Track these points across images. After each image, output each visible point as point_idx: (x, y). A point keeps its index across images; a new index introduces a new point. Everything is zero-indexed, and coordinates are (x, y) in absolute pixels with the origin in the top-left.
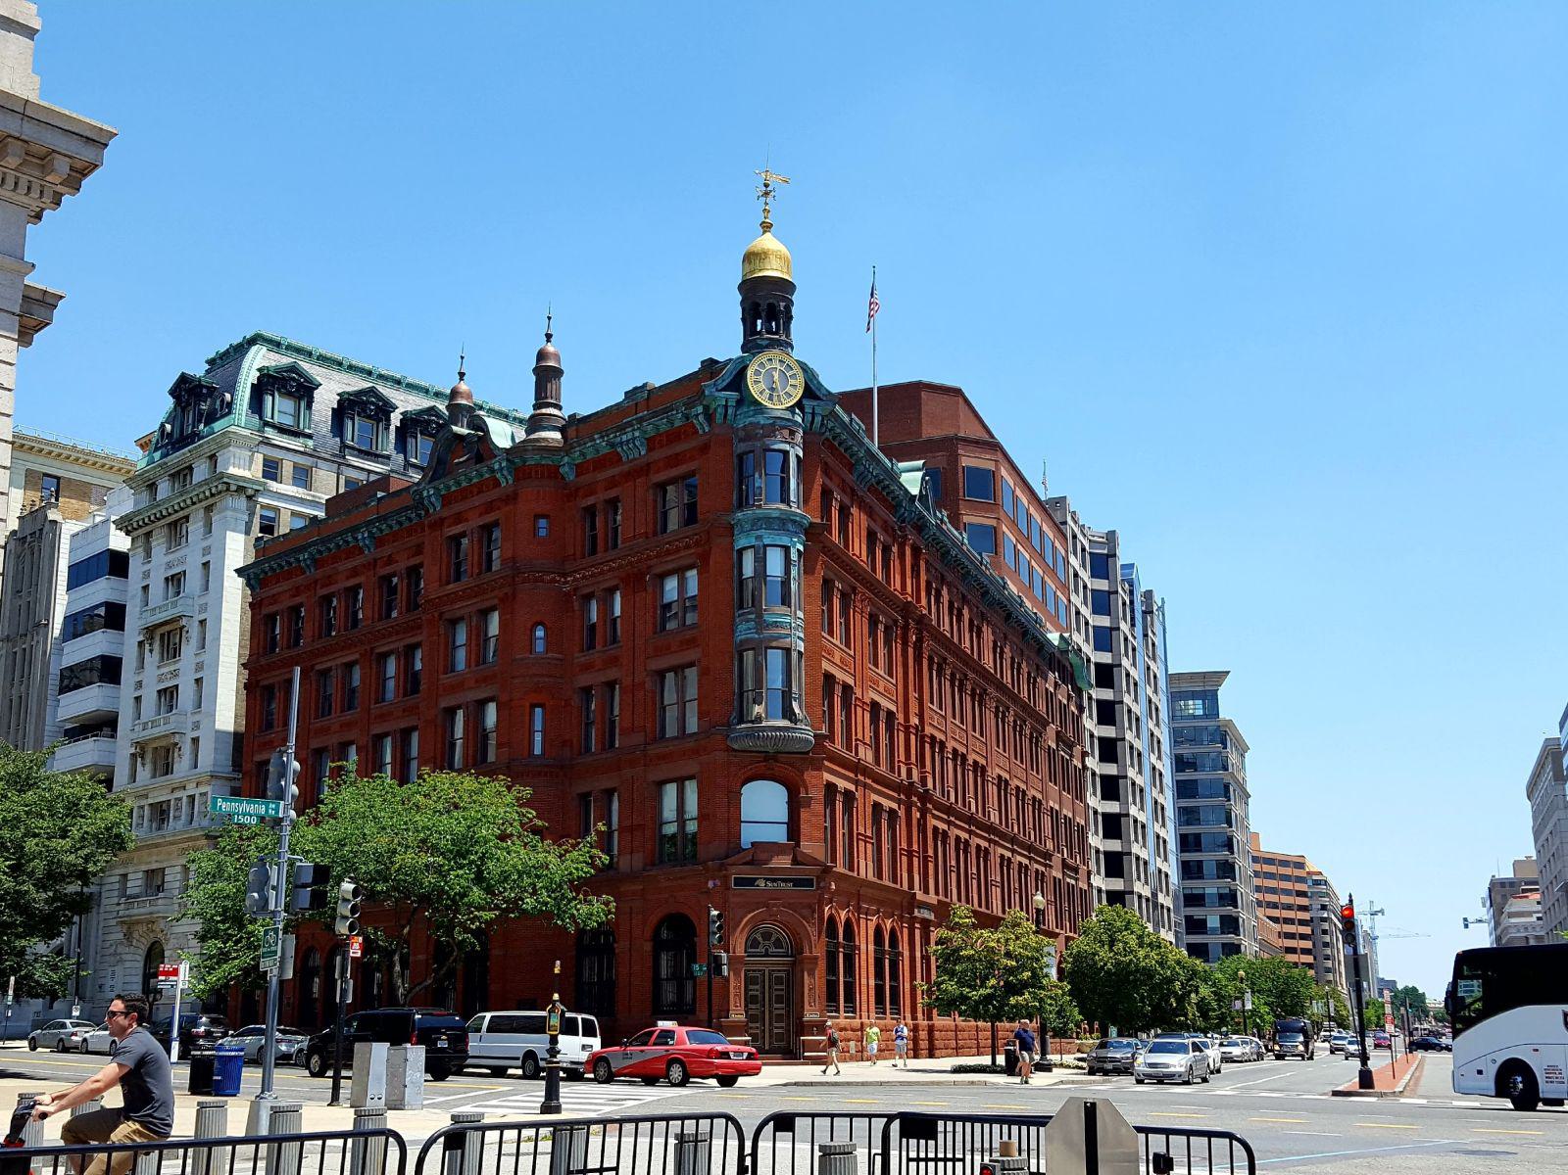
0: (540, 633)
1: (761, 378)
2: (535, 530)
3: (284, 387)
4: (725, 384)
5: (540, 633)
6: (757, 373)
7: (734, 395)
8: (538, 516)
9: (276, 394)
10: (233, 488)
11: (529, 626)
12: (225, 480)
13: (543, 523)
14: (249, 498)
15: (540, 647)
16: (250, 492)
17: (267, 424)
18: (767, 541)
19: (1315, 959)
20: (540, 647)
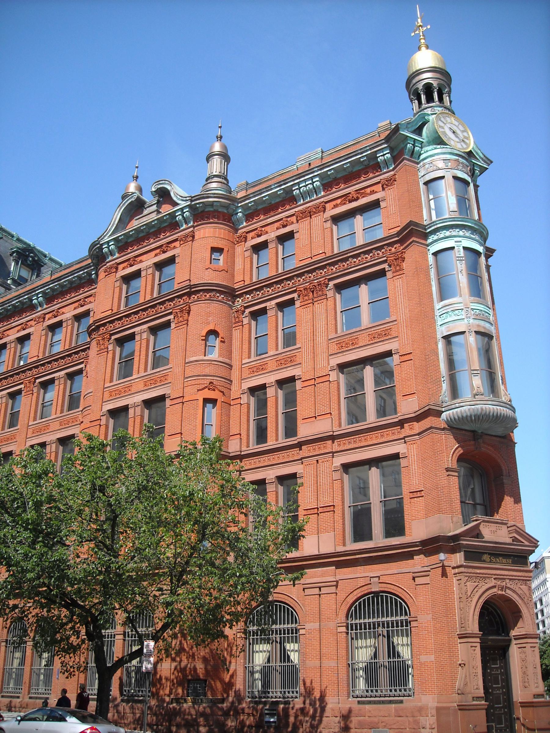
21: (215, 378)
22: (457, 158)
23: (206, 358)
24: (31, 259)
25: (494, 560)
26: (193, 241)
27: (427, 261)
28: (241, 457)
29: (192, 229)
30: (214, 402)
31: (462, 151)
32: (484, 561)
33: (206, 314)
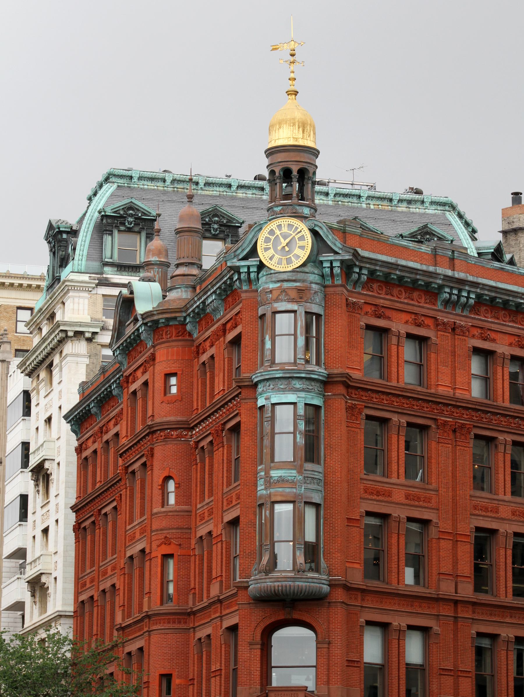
0: (171, 486)
1: (270, 245)
2: (166, 388)
3: (123, 224)
4: (245, 252)
5: (171, 486)
6: (267, 240)
7: (253, 262)
8: (168, 376)
9: (116, 232)
10: (70, 334)
11: (160, 482)
12: (62, 328)
13: (173, 381)
14: (89, 340)
15: (172, 500)
16: (88, 335)
17: (106, 264)
18: (274, 400)
20: (172, 500)
21: (170, 531)
22: (278, 285)
23: (163, 510)
24: (216, 226)
26: (154, 365)
27: (256, 417)
28: (194, 613)
29: (152, 350)
30: (171, 556)
31: (290, 269)
33: (165, 456)
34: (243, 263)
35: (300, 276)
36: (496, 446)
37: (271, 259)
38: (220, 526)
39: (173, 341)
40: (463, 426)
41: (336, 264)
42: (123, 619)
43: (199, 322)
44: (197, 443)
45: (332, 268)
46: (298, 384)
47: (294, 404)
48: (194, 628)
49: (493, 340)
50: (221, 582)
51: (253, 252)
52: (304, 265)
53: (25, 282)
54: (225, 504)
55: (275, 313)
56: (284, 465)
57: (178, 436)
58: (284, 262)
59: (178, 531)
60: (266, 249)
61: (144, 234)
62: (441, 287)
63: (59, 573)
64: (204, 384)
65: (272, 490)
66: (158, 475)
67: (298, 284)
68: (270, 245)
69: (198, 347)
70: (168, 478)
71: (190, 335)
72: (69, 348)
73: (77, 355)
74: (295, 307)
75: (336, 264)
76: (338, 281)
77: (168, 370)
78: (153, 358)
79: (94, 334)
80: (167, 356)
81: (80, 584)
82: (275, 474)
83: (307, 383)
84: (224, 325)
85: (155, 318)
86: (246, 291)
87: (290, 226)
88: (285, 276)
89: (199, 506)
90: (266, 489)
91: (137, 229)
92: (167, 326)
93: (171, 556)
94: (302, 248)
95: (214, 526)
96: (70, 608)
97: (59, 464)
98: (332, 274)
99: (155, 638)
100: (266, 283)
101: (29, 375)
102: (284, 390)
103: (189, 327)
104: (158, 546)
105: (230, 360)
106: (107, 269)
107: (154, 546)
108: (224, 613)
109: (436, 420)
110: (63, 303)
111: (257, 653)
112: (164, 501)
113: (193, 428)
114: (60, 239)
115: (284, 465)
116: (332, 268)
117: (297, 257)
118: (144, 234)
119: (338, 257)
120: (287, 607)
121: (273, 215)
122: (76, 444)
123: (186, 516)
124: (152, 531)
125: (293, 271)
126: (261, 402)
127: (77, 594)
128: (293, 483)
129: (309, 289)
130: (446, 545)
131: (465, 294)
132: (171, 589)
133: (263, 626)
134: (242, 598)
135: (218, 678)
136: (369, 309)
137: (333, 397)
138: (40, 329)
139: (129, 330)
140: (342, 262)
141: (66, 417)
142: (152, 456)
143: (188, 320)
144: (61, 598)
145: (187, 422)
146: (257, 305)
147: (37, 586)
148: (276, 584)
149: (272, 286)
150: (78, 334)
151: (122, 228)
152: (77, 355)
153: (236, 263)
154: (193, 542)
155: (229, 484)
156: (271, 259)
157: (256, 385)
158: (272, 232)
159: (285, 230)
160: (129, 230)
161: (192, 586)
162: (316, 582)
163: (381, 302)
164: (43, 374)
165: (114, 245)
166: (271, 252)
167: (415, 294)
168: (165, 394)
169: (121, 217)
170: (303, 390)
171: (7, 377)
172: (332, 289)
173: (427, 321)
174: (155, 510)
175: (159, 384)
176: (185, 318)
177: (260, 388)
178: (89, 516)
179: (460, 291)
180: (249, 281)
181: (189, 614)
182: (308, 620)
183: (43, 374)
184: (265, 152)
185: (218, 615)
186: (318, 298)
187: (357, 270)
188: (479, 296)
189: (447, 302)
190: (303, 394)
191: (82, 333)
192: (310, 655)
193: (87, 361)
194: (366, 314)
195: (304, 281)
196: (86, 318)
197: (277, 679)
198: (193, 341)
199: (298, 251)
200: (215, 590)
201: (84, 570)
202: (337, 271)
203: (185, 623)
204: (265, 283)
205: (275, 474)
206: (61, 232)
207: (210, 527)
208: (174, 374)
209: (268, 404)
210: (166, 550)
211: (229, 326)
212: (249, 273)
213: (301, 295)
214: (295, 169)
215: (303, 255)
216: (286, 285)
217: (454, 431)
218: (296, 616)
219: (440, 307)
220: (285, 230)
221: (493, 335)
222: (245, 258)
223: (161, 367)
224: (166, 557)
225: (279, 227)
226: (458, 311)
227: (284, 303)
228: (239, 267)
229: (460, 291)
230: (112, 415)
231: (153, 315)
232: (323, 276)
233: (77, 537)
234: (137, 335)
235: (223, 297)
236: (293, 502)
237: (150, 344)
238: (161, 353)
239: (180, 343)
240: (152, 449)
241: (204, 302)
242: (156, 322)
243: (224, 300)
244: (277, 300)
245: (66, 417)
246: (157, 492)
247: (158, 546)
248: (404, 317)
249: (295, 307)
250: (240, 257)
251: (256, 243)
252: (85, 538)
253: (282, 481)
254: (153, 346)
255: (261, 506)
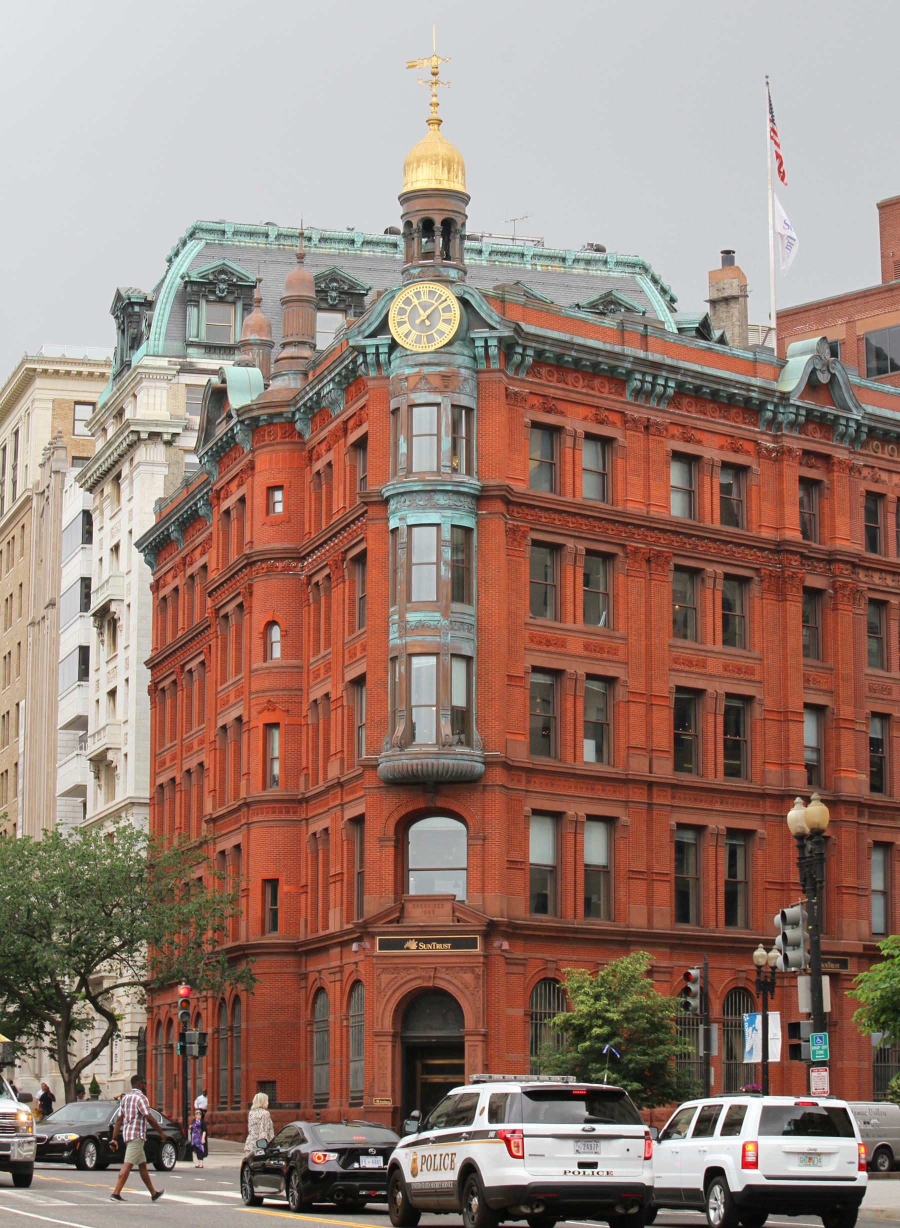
1: (405, 318)
2: (269, 506)
3: (213, 292)
6: (402, 312)
7: (383, 340)
8: (271, 489)
9: (203, 303)
10: (144, 436)
11: (262, 629)
12: (132, 428)
13: (278, 496)
14: (169, 443)
15: (277, 652)
16: (167, 437)
19: (356, 952)
20: (277, 652)
21: (275, 693)
22: (416, 370)
23: (265, 665)
24: (334, 294)
25: (424, 947)
26: (253, 475)
27: (387, 543)
28: (306, 800)
29: (250, 456)
30: (276, 725)
31: (432, 349)
32: (408, 949)
33: (268, 594)
34: (370, 342)
35: (445, 358)
36: (703, 581)
37: (407, 335)
38: (341, 687)
39: (278, 444)
40: (659, 554)
41: (493, 343)
42: (214, 808)
43: (312, 419)
44: (310, 577)
45: (486, 347)
46: (442, 500)
47: (438, 525)
48: (307, 820)
49: (699, 442)
50: (342, 759)
51: (383, 327)
52: (450, 344)
53: (85, 370)
54: (347, 656)
55: (412, 406)
56: (424, 606)
57: (287, 568)
58: (424, 340)
59: (285, 693)
60: (401, 324)
61: (239, 305)
62: (630, 373)
63: (130, 748)
64: (319, 499)
65: (409, 639)
66: (258, 619)
67: (442, 369)
68: (405, 318)
69: (310, 452)
70: (271, 624)
71: (300, 435)
72: (142, 454)
73: (153, 464)
74: (438, 399)
75: (493, 343)
76: (495, 365)
77: (272, 482)
78: (251, 466)
79: (175, 435)
80: (270, 462)
81: (157, 763)
82: (413, 617)
83: (455, 497)
84: (345, 422)
85: (255, 414)
86: (374, 378)
87: (431, 293)
88: (425, 358)
89: (312, 660)
90: (400, 637)
91: (230, 298)
92: (270, 424)
93: (276, 725)
94: (448, 321)
95: (333, 686)
96: (145, 794)
97: (129, 606)
98: (487, 357)
99: (256, 832)
100: (400, 367)
101: (91, 490)
102: (424, 507)
103: (298, 426)
104: (259, 713)
105: (353, 468)
106: (191, 350)
107: (254, 713)
108: (346, 800)
109: (623, 546)
110: (135, 396)
111: (390, 851)
112: (266, 654)
113: (304, 558)
114: (130, 313)
115: (424, 606)
116: (486, 347)
117: (441, 333)
118: (239, 305)
119: (495, 334)
120: (429, 792)
121: (409, 279)
122: (151, 579)
123: (296, 674)
124: (250, 693)
125: (436, 352)
126: (392, 524)
127: (154, 775)
128: (436, 630)
129: (456, 375)
130: (637, 710)
131: (661, 381)
132: (277, 769)
133: (397, 816)
134: (369, 781)
135: (338, 884)
136: (536, 401)
137: (489, 516)
138: (105, 430)
139: (220, 430)
140: (500, 339)
141: (138, 545)
142: (251, 594)
143: (297, 416)
144: (134, 780)
145: (296, 551)
146: (387, 396)
147: (102, 764)
148: (415, 762)
149: (407, 371)
150: (154, 436)
151: (212, 298)
152: (153, 464)
153: (361, 341)
154: (305, 707)
155: (352, 631)
156: (407, 336)
157: (386, 501)
158: (408, 301)
159: (425, 298)
160: (221, 300)
161: (304, 765)
162: (467, 758)
163: (552, 392)
164: (108, 489)
165: (203, 319)
166: (407, 327)
167: (597, 382)
168: (268, 513)
169: (210, 283)
170: (449, 507)
171: (62, 492)
172: (486, 375)
173: (614, 417)
174: (255, 666)
175: (259, 500)
176: (294, 414)
177: (393, 505)
178: (170, 672)
179: (655, 377)
180: (378, 365)
181: (300, 801)
182: (456, 809)
183: (108, 489)
184: (399, 199)
185: (338, 802)
186: (470, 387)
187: (520, 350)
188: (680, 385)
189: (638, 393)
190: (449, 513)
191: (159, 434)
192: (459, 855)
193: (165, 471)
194: (532, 407)
195: (450, 365)
196: (165, 416)
197: (416, 885)
198: (304, 443)
199: (442, 326)
200: (334, 770)
201: (162, 744)
202: (493, 351)
203: (295, 812)
204: (398, 368)
205: (413, 617)
206: (132, 304)
207: (327, 688)
208: (280, 488)
209: (403, 526)
210: (271, 718)
211: (351, 424)
212: (377, 354)
213: (447, 382)
214: (438, 220)
215: (450, 331)
216: (426, 370)
217: (648, 561)
218: (440, 803)
219: (629, 398)
220: (425, 298)
221: (698, 435)
222: (373, 335)
223: (262, 479)
224: (270, 726)
225: (418, 294)
226: (653, 403)
227: (424, 394)
228: (364, 347)
229: (655, 377)
230: (197, 542)
231: (251, 410)
232: (475, 358)
233: (153, 702)
234: (231, 437)
235: (344, 386)
236: (437, 654)
237: (247, 448)
238: (263, 459)
239: (287, 447)
240: (251, 586)
241: (318, 393)
242: (256, 419)
243: (345, 390)
244: (414, 389)
245: (138, 545)
246: (257, 642)
247: (259, 713)
248: (582, 411)
249: (438, 399)
250: (367, 334)
251: (387, 315)
252: (163, 703)
253: (421, 627)
254: (252, 451)
255: (394, 659)
